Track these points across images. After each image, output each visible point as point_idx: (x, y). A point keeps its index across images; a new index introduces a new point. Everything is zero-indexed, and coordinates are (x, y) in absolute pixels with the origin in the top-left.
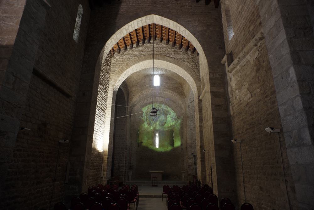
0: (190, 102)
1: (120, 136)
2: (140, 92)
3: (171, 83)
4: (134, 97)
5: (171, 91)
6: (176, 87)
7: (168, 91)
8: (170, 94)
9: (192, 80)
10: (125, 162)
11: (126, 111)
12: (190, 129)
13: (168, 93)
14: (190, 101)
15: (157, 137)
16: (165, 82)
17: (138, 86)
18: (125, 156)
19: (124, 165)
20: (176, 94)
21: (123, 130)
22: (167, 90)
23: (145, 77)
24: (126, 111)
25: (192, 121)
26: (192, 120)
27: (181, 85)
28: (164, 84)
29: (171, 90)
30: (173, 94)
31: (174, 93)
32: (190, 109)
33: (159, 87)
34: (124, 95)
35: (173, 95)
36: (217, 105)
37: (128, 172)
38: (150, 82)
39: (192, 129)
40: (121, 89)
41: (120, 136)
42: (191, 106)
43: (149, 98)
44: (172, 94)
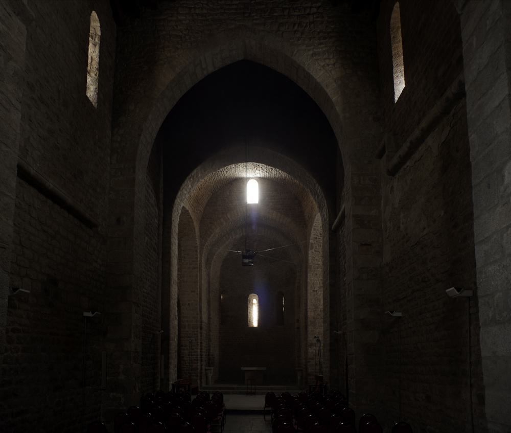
9: (318, 191)
11: (199, 255)
18: (199, 341)
19: (199, 357)
21: (194, 292)
24: (197, 255)
36: (363, 243)
37: (206, 370)
40: (188, 211)
41: (189, 304)
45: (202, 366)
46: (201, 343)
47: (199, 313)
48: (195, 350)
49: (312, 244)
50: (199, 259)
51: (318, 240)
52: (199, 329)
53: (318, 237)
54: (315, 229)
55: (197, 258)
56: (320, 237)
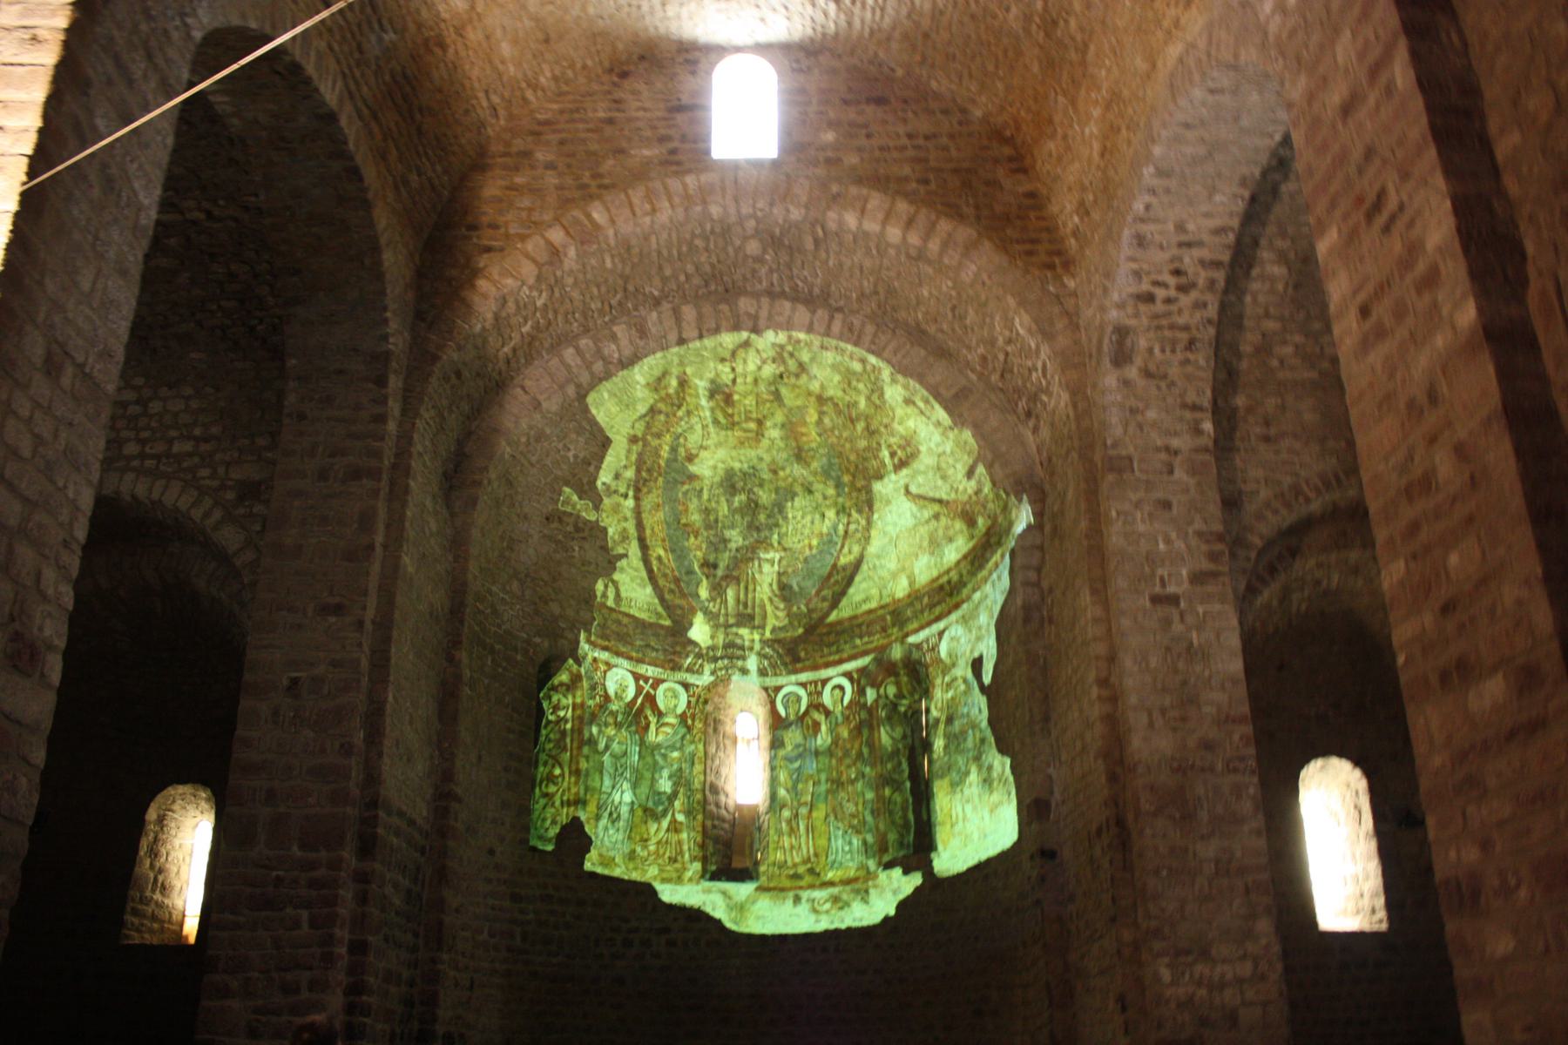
0: (1133, 289)
2: (557, 219)
3: (901, 130)
4: (495, 271)
5: (903, 206)
6: (956, 171)
7: (876, 201)
8: (894, 234)
10: (350, 1009)
11: (394, 407)
12: (1156, 600)
13: (872, 226)
14: (1137, 275)
16: (832, 125)
17: (541, 156)
18: (342, 933)
20: (965, 233)
21: (338, 609)
22: (854, 190)
23: (624, 75)
24: (383, 401)
25: (1167, 505)
26: (1160, 495)
27: (1007, 151)
28: (829, 136)
29: (910, 197)
30: (927, 236)
31: (944, 226)
32: (1132, 372)
33: (775, 164)
34: (367, 205)
35: (934, 246)
38: (680, 118)
39: (1173, 600)
42: (1143, 343)
43: (657, 302)
44: (914, 239)
46: (359, 948)
47: (359, 737)
48: (305, 994)
50: (392, 426)
51: (1159, 307)
52: (348, 855)
53: (1160, 293)
54: (1141, 241)
55: (381, 419)
56: (1173, 293)
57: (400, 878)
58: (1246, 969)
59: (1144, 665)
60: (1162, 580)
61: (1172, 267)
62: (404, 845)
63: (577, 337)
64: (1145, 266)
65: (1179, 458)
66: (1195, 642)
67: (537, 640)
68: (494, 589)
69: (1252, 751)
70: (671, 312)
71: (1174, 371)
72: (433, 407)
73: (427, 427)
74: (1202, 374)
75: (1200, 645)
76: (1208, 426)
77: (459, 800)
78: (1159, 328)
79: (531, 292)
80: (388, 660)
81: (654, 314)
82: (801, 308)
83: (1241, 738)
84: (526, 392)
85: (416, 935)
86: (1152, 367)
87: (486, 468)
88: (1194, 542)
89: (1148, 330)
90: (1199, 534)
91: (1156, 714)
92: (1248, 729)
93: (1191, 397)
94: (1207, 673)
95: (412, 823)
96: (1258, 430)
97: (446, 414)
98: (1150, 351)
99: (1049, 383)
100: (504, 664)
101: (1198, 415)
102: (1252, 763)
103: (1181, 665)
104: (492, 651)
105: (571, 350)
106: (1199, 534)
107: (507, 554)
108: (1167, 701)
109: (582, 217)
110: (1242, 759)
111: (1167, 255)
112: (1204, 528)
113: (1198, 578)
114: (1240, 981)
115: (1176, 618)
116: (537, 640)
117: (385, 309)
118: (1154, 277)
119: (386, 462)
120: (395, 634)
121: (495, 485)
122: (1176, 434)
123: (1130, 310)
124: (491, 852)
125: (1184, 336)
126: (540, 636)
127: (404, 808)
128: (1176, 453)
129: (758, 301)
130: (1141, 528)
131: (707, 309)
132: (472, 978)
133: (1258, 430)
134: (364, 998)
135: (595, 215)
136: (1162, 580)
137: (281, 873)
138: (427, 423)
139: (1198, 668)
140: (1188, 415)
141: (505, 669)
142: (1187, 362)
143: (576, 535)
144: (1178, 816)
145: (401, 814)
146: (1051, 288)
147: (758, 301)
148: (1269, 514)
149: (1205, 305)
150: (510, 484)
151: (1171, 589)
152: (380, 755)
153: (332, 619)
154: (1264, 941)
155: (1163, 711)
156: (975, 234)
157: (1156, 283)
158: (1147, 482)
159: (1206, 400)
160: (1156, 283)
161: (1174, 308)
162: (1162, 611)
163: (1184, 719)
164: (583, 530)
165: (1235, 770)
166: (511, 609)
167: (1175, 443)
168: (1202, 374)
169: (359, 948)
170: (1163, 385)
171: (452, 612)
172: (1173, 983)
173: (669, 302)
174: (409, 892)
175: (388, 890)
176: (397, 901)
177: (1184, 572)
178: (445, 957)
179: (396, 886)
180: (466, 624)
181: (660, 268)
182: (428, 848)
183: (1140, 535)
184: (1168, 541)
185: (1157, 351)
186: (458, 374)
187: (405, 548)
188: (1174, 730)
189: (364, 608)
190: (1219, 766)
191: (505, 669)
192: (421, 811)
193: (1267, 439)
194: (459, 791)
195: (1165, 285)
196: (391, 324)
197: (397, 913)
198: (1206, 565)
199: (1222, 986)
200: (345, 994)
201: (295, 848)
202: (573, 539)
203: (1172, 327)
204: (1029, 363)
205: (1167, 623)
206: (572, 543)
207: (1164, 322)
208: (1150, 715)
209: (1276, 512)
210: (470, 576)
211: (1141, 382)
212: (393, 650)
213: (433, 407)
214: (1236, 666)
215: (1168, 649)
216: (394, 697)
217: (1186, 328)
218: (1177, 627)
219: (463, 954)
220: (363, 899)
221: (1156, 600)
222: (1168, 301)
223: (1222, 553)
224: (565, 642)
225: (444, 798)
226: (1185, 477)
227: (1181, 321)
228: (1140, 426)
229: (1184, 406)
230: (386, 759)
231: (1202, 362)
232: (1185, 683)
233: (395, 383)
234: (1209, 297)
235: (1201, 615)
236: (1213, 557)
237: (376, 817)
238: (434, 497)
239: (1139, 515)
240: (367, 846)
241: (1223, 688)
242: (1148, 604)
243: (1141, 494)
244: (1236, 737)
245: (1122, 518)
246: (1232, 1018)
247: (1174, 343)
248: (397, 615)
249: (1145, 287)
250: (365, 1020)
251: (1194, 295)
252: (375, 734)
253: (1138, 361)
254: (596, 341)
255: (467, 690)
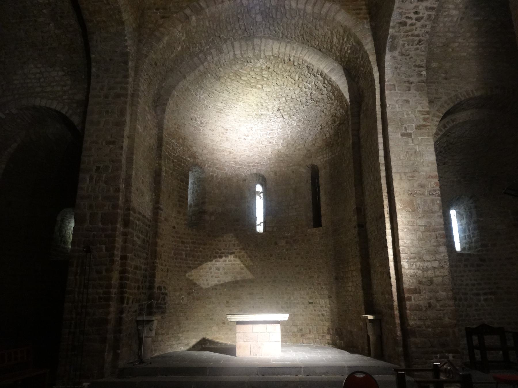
0: (399, 21)
1: (98, 168)
10: (121, 279)
11: (131, 73)
13: (301, 6)
14: (401, 14)
15: (258, 197)
18: (118, 253)
21: (113, 143)
26: (405, 98)
32: (396, 53)
39: (410, 135)
41: (98, 168)
42: (401, 42)
43: (225, 41)
45: (121, 312)
46: (124, 258)
47: (122, 186)
49: (394, 38)
50: (130, 79)
53: (409, 22)
55: (126, 77)
56: (413, 21)
57: (140, 235)
58: (436, 264)
59: (398, 158)
60: (405, 128)
61: (415, 10)
62: (141, 224)
63: (198, 54)
64: (404, 11)
65: (413, 85)
66: (418, 150)
67: (189, 159)
68: (173, 141)
69: (438, 188)
70: (231, 44)
71: (412, 53)
72: (147, 74)
73: (145, 81)
74: (423, 53)
75: (419, 151)
76: (424, 73)
77: (162, 210)
78: (407, 36)
79: (180, 34)
80: (132, 160)
81: (225, 45)
82: (276, 42)
83: (435, 183)
84: (181, 73)
85: (147, 254)
86: (404, 51)
87: (168, 99)
88: (417, 115)
89: (403, 37)
90: (420, 111)
91: (403, 175)
92: (437, 180)
93: (418, 63)
94: (422, 160)
95: (144, 217)
96: (443, 75)
97: (152, 78)
98: (403, 45)
99: (364, 63)
100: (177, 166)
101: (421, 69)
102: (439, 192)
103: (412, 158)
104: (173, 162)
105: (196, 58)
106: (420, 111)
107: (177, 130)
108: (407, 171)
109: (197, 5)
110: (435, 191)
111: (412, 6)
112: (422, 110)
113: (419, 127)
114: (434, 268)
115: (411, 141)
116: (189, 159)
117: (125, 36)
118: (407, 15)
119: (129, 92)
120: (135, 152)
121: (172, 105)
122: (412, 76)
123: (397, 29)
124: (174, 227)
125: (417, 38)
126: (190, 158)
127: (141, 211)
128: (412, 83)
129: (261, 40)
130: (398, 110)
131: (243, 43)
132: (168, 269)
133: (443, 75)
134: (126, 275)
135: (201, 4)
136: (405, 128)
137: (95, 233)
138: (145, 80)
139: (419, 159)
140: (417, 69)
141: (178, 168)
142: (417, 49)
143: (201, 125)
144: (410, 210)
145: (140, 213)
146: (366, 27)
147: (261, 40)
148: (446, 106)
149: (426, 26)
150: (177, 105)
151: (408, 131)
152: (130, 192)
153: (111, 146)
154: (443, 255)
155: (405, 174)
156: (338, 8)
157: (408, 18)
158: (401, 93)
159: (424, 64)
160: (408, 18)
161: (414, 27)
162: (406, 139)
163: (413, 177)
164: (204, 123)
165: (433, 194)
166: (179, 148)
167: (411, 79)
168: (423, 53)
169: (124, 258)
170: (408, 58)
171: (158, 148)
172: (408, 269)
173: (230, 41)
174: (144, 240)
175: (135, 238)
176: (139, 242)
177: (414, 125)
178: (158, 261)
179: (138, 237)
180: (163, 152)
181: (226, 27)
182: (151, 226)
183: (398, 112)
184: (408, 115)
185: (406, 45)
186: (156, 64)
187: (138, 122)
188: (410, 180)
189: (123, 142)
190: (426, 193)
191: (178, 168)
192: (149, 214)
193: (446, 79)
194: (162, 207)
195: (410, 18)
196: (128, 41)
197: (139, 246)
198: (422, 122)
199: (427, 270)
200: (119, 274)
201: (100, 224)
202: (200, 126)
203: (412, 35)
204: (356, 56)
205: (407, 143)
206: (200, 128)
207: (410, 33)
208: (400, 175)
209: (448, 104)
210: (164, 136)
211: (399, 58)
212: (134, 157)
213: (147, 74)
214: (433, 158)
215: (407, 152)
216: (135, 173)
217: (418, 36)
218: (411, 144)
219: (164, 261)
220: (125, 241)
221: (403, 135)
222: (412, 25)
223: (428, 118)
224: (199, 160)
225: (156, 209)
226: (415, 92)
227: (416, 33)
228: (398, 74)
229: (415, 66)
230: (132, 194)
231: (423, 49)
232: (413, 164)
233: (131, 64)
234: (427, 23)
235: (420, 140)
236: (425, 120)
237: (129, 213)
238: (149, 107)
239: (397, 106)
240: (126, 223)
241: (428, 166)
242: (400, 137)
243: (398, 98)
244: (433, 183)
245: (391, 106)
246: (431, 281)
247: (413, 41)
248: (135, 145)
249: (404, 19)
250: (127, 282)
251: (422, 22)
252: (128, 185)
253: (399, 49)
254: (205, 55)
255: (164, 174)
